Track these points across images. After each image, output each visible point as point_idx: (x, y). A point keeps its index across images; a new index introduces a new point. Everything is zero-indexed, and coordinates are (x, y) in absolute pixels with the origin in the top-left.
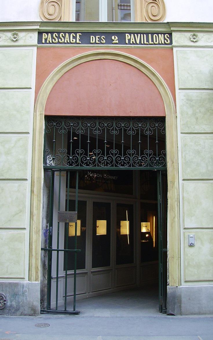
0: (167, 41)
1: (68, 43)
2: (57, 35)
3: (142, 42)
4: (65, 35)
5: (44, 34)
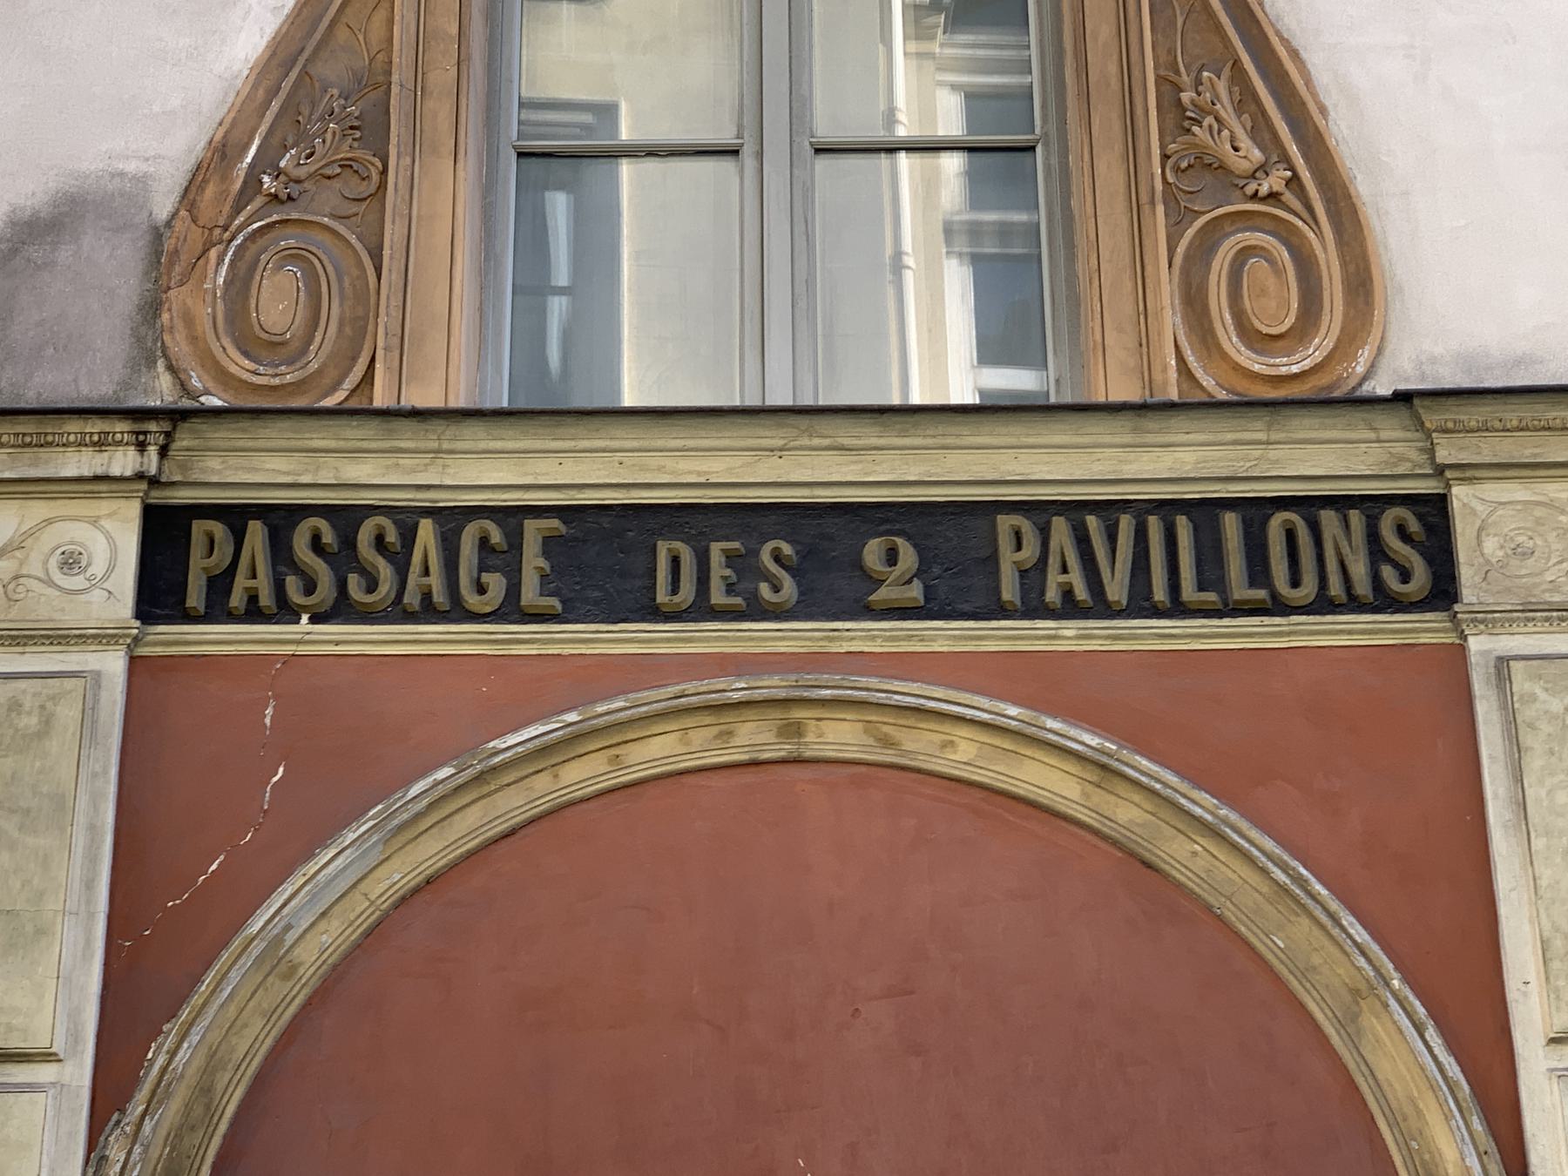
0: (1405, 576)
1: (428, 612)
2: (328, 537)
3: (1160, 594)
4: (409, 535)
5: (199, 527)
